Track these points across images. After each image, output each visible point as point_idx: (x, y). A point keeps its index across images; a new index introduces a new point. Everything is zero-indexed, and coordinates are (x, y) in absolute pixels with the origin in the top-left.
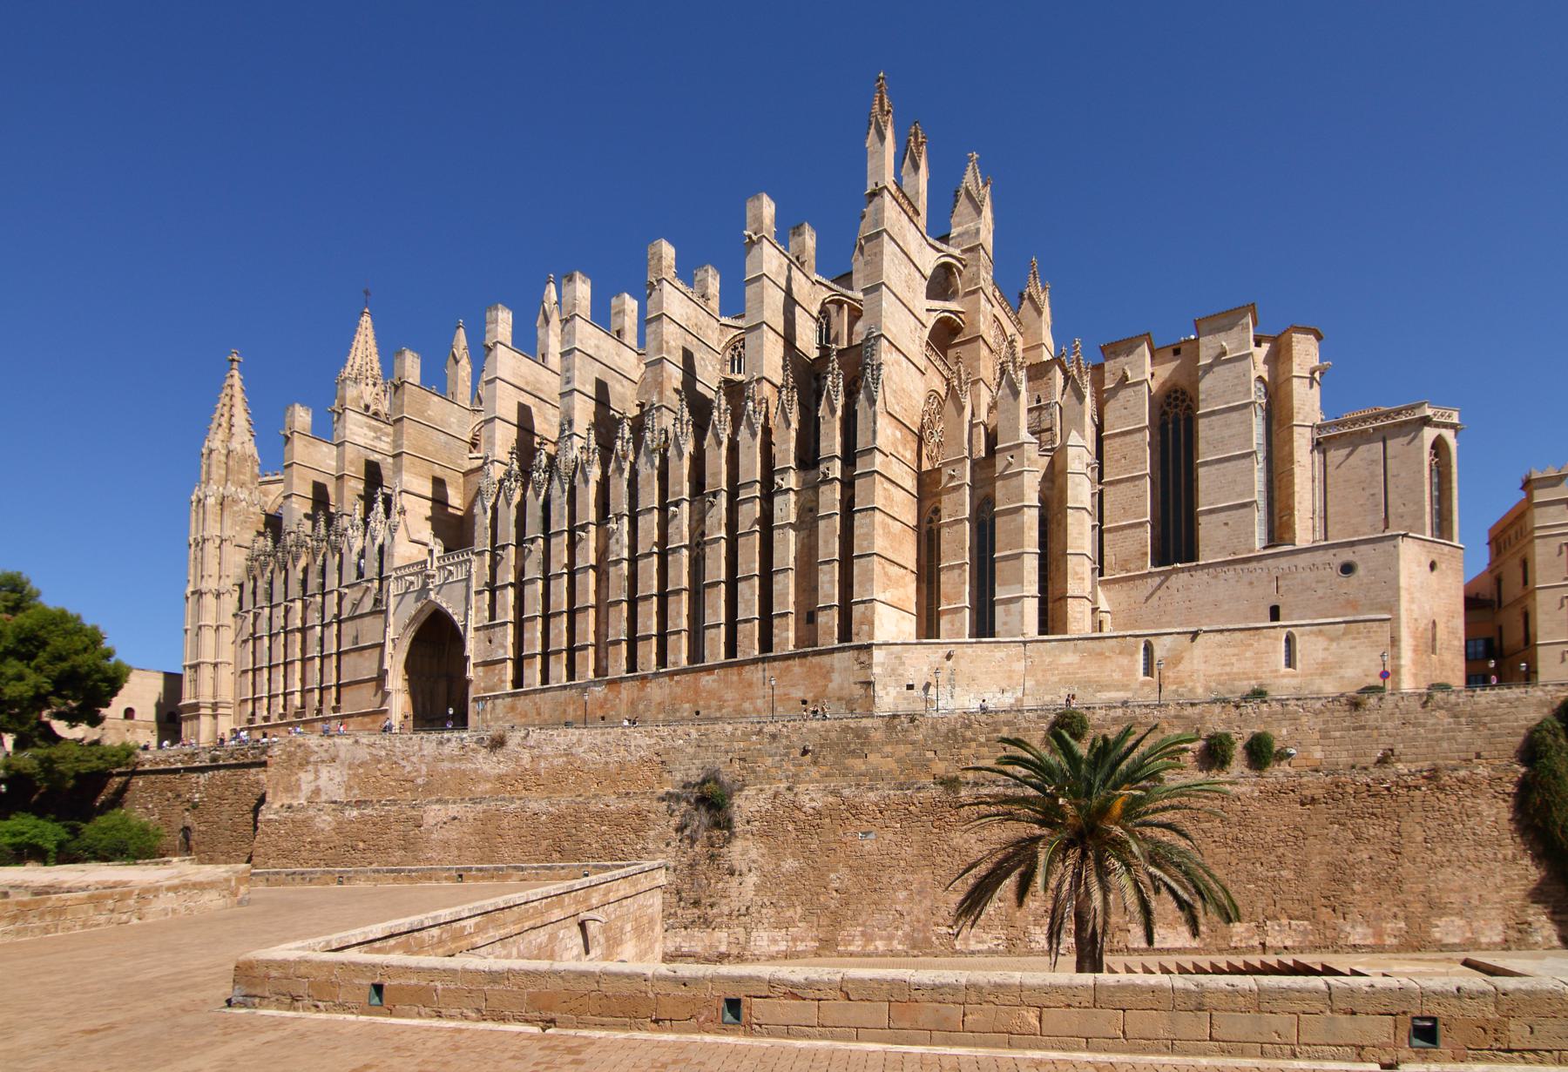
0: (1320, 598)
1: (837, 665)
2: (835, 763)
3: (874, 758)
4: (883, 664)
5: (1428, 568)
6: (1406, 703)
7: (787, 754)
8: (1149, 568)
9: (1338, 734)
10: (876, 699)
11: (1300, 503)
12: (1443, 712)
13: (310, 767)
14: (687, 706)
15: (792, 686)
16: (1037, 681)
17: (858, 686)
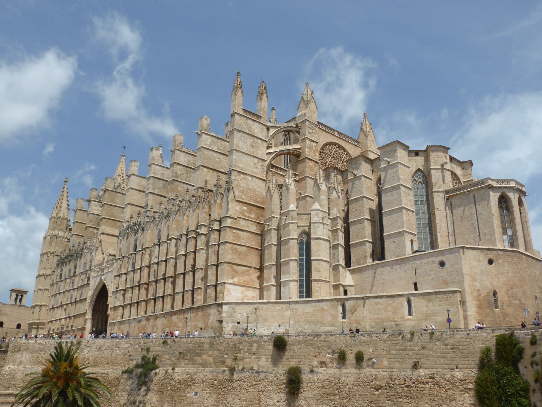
0: (432, 279)
1: (212, 312)
2: (191, 358)
3: (205, 357)
4: (227, 312)
5: (487, 263)
6: (424, 337)
7: (173, 354)
8: (369, 261)
9: (394, 352)
10: (224, 329)
11: (440, 229)
12: (440, 342)
13: (20, 352)
14: (168, 329)
15: (198, 321)
16: (295, 321)
17: (218, 322)
